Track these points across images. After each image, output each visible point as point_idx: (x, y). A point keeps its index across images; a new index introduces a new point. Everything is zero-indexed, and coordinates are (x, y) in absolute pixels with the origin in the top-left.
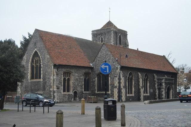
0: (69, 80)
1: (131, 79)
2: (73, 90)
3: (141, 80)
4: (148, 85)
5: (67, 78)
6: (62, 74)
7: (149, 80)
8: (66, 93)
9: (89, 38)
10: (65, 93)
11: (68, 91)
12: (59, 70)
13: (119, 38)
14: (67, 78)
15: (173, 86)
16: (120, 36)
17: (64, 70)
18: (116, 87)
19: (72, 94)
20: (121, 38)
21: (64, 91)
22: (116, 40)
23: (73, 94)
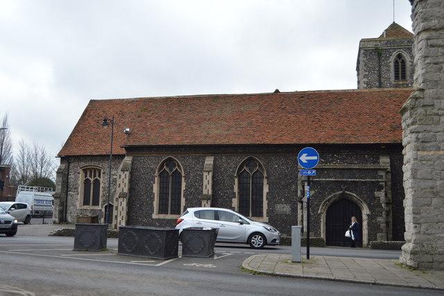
0: (97, 183)
1: (177, 176)
2: (104, 202)
3: (208, 179)
4: (266, 190)
5: (92, 180)
6: (79, 173)
7: (265, 175)
8: (90, 207)
9: (347, 80)
10: (85, 207)
11: (96, 203)
12: (72, 165)
13: (392, 64)
14: (92, 180)
15: (381, 195)
16: (400, 56)
17: (83, 164)
18: (122, 195)
19: (100, 210)
20: (403, 62)
21: (86, 202)
22: (379, 71)
23: (103, 210)
